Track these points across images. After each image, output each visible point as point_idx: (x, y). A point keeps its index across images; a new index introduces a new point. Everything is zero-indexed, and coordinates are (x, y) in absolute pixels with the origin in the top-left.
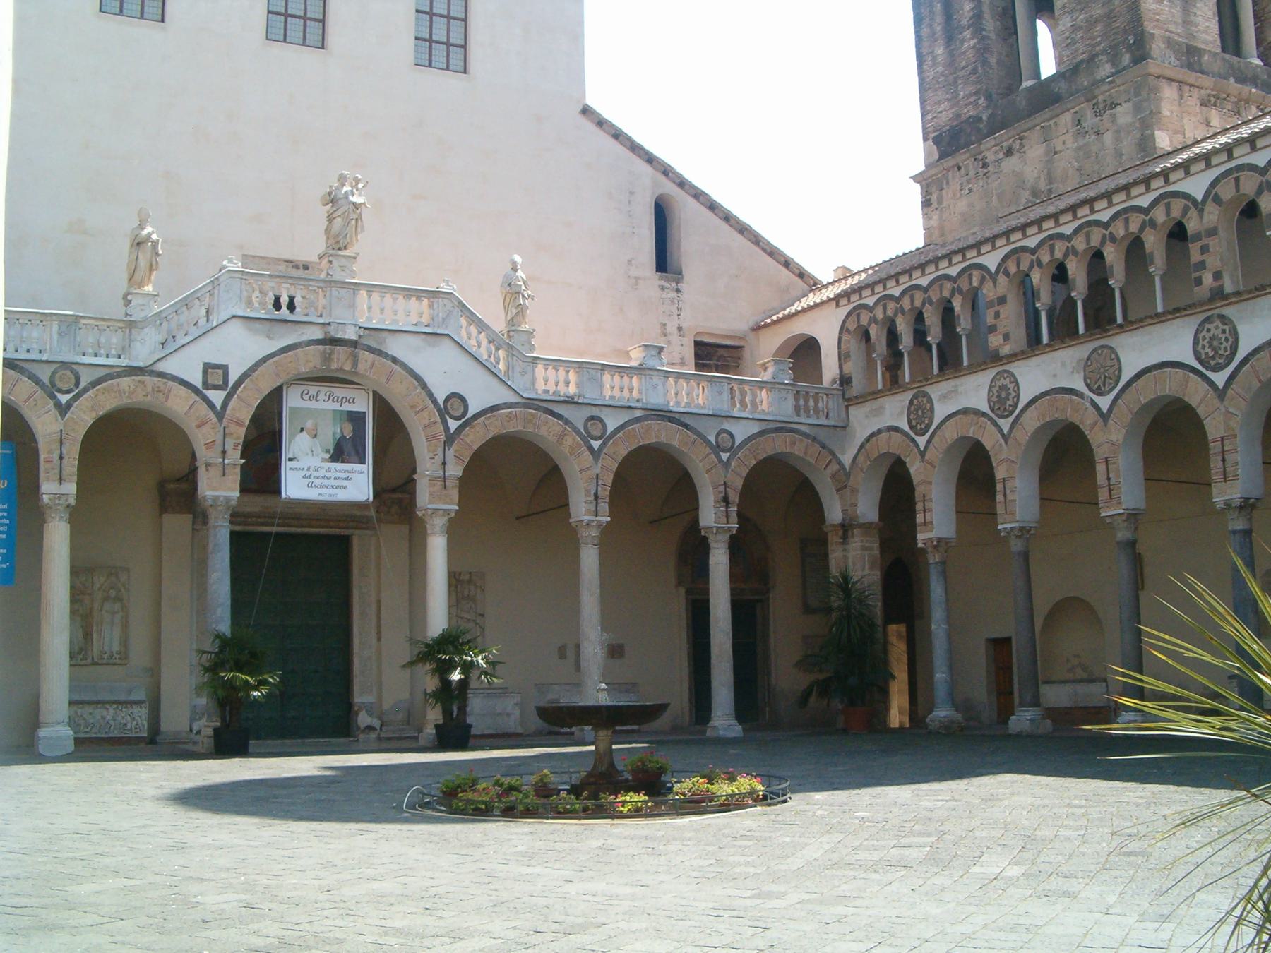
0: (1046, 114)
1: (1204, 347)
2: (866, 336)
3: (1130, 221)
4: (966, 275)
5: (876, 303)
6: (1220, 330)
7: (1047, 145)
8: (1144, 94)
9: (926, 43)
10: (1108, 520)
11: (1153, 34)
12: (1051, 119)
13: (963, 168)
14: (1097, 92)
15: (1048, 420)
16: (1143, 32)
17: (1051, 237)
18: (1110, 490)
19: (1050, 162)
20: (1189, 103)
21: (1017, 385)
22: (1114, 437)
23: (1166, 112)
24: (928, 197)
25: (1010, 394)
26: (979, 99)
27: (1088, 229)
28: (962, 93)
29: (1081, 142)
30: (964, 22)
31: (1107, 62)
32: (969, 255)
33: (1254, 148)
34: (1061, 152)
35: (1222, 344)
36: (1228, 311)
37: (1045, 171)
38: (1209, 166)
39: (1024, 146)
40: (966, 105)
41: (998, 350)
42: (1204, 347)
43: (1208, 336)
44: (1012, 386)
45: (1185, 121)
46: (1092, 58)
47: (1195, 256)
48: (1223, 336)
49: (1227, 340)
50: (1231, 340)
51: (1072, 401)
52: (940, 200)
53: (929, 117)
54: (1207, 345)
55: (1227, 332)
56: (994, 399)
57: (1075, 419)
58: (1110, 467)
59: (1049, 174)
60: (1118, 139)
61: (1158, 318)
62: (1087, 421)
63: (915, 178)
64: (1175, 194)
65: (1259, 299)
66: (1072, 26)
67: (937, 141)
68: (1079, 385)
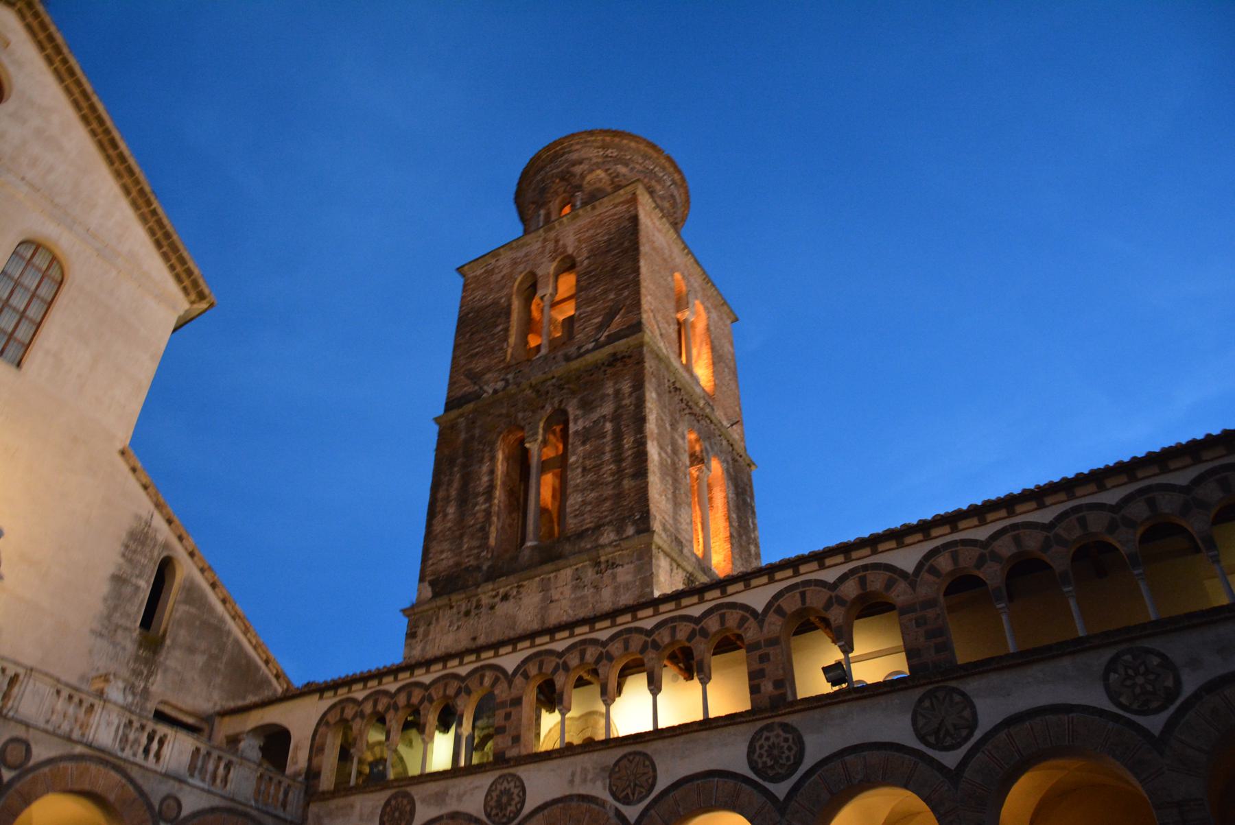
0: (549, 567)
1: (761, 756)
3: (678, 630)
4: (477, 676)
5: (366, 699)
6: (782, 739)
7: (544, 595)
8: (646, 559)
9: (439, 504)
12: (552, 572)
13: (455, 607)
14: (601, 552)
16: (648, 512)
17: (583, 642)
24: (413, 630)
25: (513, 799)
26: (483, 551)
27: (628, 636)
28: (465, 546)
29: (579, 594)
30: (481, 489)
31: (613, 531)
32: (484, 655)
33: (822, 567)
34: (557, 601)
35: (783, 753)
36: (788, 719)
37: (539, 616)
38: (772, 580)
39: (521, 593)
40: (468, 556)
41: (504, 753)
42: (761, 756)
43: (766, 745)
44: (516, 791)
46: (598, 528)
48: (786, 745)
49: (790, 749)
50: (795, 748)
52: (426, 634)
53: (430, 562)
54: (765, 754)
55: (791, 740)
56: (493, 803)
63: (404, 611)
64: (733, 606)
66: (582, 501)
67: (432, 584)
68: (605, 796)
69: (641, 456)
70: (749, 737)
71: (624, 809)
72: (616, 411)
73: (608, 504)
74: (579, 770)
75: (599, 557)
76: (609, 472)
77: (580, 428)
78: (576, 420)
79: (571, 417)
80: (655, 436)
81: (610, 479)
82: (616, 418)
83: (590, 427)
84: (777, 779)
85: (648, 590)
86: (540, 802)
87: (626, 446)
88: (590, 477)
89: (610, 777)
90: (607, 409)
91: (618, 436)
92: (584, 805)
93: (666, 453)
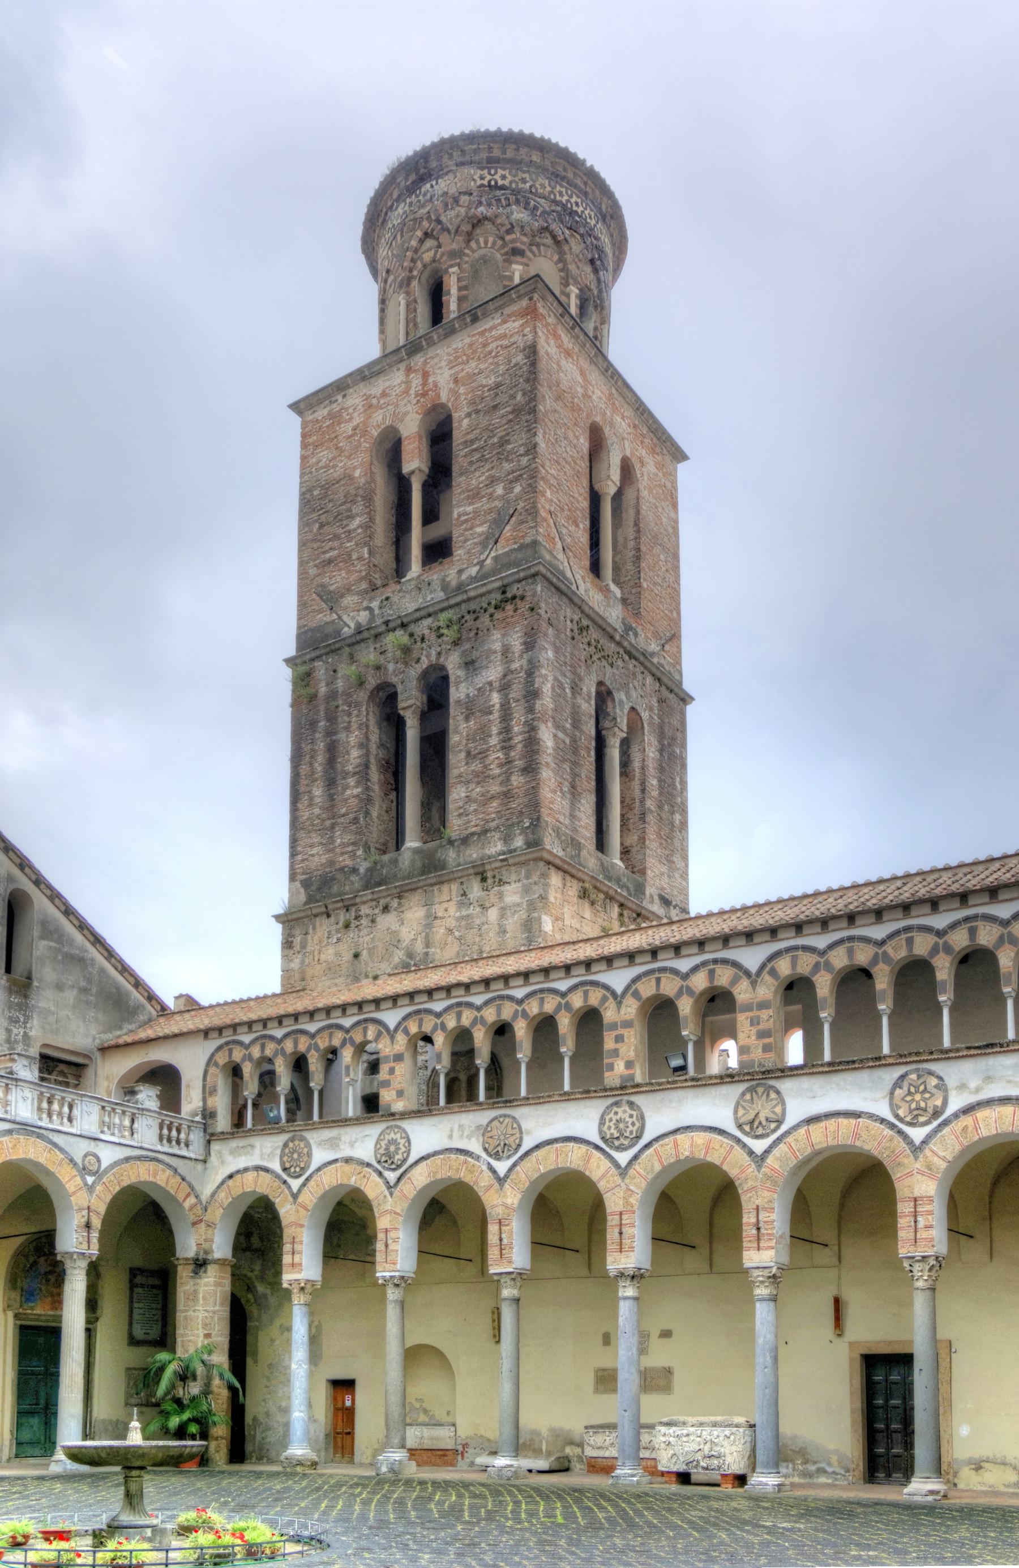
1: (609, 1128)
2: (236, 1072)
4: (360, 1029)
10: (496, 1278)
11: (547, 822)
15: (439, 1177)
16: (538, 819)
18: (501, 1249)
19: (428, 926)
20: (570, 893)
21: (409, 1141)
22: (509, 1201)
23: (552, 899)
25: (399, 1149)
31: (500, 839)
36: (634, 1099)
42: (609, 1128)
43: (614, 1118)
44: (402, 1141)
45: (566, 910)
46: (486, 832)
47: (609, 1044)
48: (630, 1121)
50: (637, 1125)
51: (465, 1162)
57: (468, 1179)
58: (503, 1228)
59: (427, 936)
60: (502, 916)
61: (568, 1097)
62: (481, 1181)
65: (667, 1093)
69: (532, 743)
70: (601, 1110)
71: (495, 1164)
72: (505, 676)
73: (495, 804)
74: (456, 1126)
75: (485, 871)
76: (497, 762)
77: (463, 696)
78: (458, 683)
79: (452, 679)
80: (550, 713)
81: (497, 771)
82: (505, 688)
83: (474, 696)
84: (621, 1148)
85: (535, 915)
86: (423, 1153)
87: (516, 729)
88: (476, 766)
89: (483, 1135)
90: (493, 673)
91: (506, 716)
92: (462, 1158)
93: (564, 730)
